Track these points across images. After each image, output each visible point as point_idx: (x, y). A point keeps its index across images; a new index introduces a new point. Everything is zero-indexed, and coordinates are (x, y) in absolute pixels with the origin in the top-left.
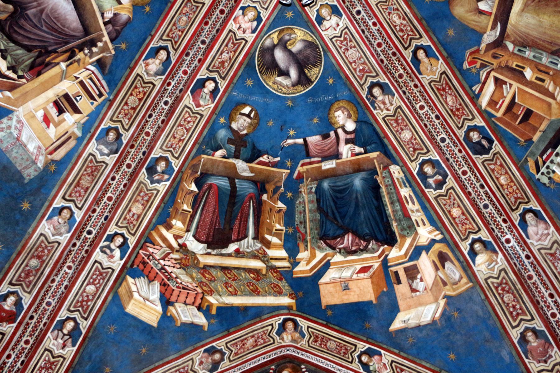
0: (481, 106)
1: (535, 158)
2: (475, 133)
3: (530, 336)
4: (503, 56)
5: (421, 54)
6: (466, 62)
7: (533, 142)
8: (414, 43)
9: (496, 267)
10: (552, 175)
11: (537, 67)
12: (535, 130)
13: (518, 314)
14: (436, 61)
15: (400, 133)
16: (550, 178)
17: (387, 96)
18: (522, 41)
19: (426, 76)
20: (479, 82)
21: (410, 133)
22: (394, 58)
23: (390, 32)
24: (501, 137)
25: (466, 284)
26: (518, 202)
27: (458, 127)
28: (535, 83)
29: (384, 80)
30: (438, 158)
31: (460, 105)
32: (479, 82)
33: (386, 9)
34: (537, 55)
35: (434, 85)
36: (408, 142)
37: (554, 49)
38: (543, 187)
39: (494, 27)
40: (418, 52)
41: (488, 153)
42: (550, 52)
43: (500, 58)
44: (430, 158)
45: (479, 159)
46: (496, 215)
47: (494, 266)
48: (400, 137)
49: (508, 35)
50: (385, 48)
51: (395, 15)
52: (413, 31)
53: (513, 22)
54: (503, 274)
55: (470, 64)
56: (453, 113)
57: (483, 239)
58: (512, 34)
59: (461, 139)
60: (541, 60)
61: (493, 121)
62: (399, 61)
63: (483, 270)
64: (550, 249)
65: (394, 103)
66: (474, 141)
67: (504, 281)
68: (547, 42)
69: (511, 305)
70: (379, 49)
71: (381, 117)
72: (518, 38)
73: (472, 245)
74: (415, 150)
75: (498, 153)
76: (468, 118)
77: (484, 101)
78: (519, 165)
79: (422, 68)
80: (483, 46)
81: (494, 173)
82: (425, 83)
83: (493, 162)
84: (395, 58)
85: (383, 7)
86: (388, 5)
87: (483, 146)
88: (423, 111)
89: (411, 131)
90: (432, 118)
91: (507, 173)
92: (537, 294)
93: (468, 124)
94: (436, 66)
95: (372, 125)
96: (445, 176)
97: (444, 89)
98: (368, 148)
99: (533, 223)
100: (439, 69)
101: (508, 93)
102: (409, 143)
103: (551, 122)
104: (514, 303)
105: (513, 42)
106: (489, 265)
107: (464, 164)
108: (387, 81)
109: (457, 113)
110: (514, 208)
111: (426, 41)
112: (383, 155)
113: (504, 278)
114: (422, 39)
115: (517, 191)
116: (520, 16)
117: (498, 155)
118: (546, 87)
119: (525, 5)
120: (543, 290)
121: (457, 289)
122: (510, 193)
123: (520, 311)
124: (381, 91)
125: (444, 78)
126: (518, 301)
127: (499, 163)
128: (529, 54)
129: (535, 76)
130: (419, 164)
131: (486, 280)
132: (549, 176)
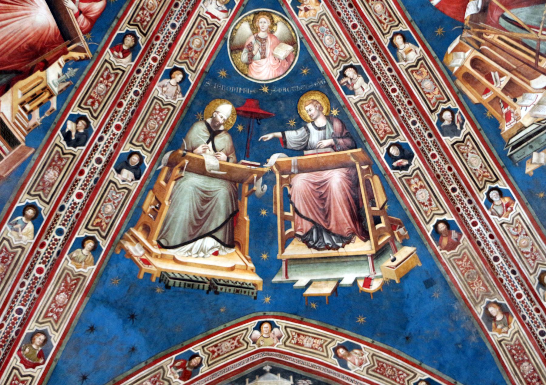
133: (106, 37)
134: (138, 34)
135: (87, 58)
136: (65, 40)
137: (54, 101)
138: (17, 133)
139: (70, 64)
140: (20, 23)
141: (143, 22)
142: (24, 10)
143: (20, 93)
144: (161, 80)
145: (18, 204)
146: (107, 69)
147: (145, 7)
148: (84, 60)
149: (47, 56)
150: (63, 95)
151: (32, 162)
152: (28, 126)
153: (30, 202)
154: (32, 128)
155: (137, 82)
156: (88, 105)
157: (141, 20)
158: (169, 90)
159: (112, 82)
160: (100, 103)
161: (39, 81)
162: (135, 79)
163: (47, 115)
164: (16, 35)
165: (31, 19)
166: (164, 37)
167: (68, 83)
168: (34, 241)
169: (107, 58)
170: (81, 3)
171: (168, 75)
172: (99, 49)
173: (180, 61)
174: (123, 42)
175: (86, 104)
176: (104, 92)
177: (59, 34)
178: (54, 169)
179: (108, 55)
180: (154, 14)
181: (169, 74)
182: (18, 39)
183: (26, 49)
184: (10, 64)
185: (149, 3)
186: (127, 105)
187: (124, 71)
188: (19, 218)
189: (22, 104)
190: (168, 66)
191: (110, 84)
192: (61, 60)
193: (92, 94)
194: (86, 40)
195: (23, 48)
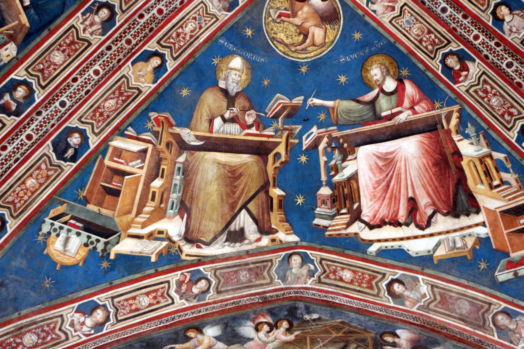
0: (111, 141)
1: (68, 212)
2: (80, 139)
4: (171, 153)
5: (156, 62)
6: (157, 115)
7: (86, 206)
8: (166, 52)
10: (53, 234)
11: (165, 191)
12: (100, 204)
14: (151, 81)
15: (58, 50)
16: (49, 233)
17: (100, 27)
18: (189, 169)
19: (132, 70)
20: (138, 133)
21: (61, 62)
22: (147, 30)
23: (174, 21)
24: (82, 169)
26: (9, 206)
27: (81, 117)
28: (149, 192)
29: (119, 21)
30: (38, 101)
31: (108, 116)
32: (138, 133)
33: (199, 15)
34: (178, 187)
35: (124, 82)
36: (50, 62)
37: (187, 203)
38: (37, 228)
39: (198, 138)
40: (158, 58)
41: (58, 158)
42: (183, 200)
43: (168, 150)
44: (35, 92)
45: (47, 148)
48: (53, 50)
49: (193, 154)
50: (157, 18)
51: (194, 25)
52: (179, 48)
53: (206, 157)
55: (156, 119)
56: (96, 110)
58: (195, 158)
59: (67, 124)
60: (174, 192)
61: (98, 157)
62: (144, 37)
65: (94, 36)
66: (68, 139)
68: (193, 194)
70: (155, 11)
71: (74, 23)
72: (192, 165)
74: (42, 71)
75: (63, 170)
76: (95, 128)
77: (118, 143)
78: (54, 196)
79: (140, 64)
80: (177, 130)
81: (36, 170)
82: (124, 70)
83: (49, 167)
84: (148, 32)
85: (201, 10)
86: (204, 16)
87: (65, 151)
88: (92, 75)
89: (64, 63)
90: (86, 87)
91: (41, 185)
93: (87, 129)
94: (146, 81)
95: (62, 13)
96: (17, 114)
97: (121, 94)
98: (32, 11)
100: (143, 86)
101: (133, 167)
102: (49, 63)
103: (111, 218)
105: (186, 160)
107: (39, 134)
108: (118, 24)
109: (97, 114)
111: (171, 65)
112: (27, 31)
114: (172, 60)
115: (22, 202)
116: (214, 162)
117: (59, 171)
118: (148, 204)
119: (225, 165)
122: (18, 194)
124: (106, 18)
125: (135, 93)
127: (50, 173)
128: (178, 179)
129: (156, 190)
130: (25, 79)
132: (52, 231)
133: (442, 86)
134: (447, 50)
135: (460, 111)
136: (437, 129)
137: (497, 155)
138: (520, 201)
139: (462, 130)
140: (412, 168)
141: (434, 42)
142: (401, 161)
143: (480, 186)
144: (503, 32)
146: (476, 92)
147: (419, 38)
148: (460, 115)
149: (449, 150)
150: (493, 144)
152: (516, 187)
154: (520, 184)
155: (498, 62)
156: (511, 120)
157: (432, 45)
158: (516, 25)
159: (492, 88)
160: (512, 106)
161: (472, 164)
162: (494, 63)
163: (509, 166)
164: (422, 175)
165: (410, 158)
166: (454, 23)
167: (481, 136)
169: (464, 89)
170: (404, 106)
171: (500, 23)
172: (453, 96)
173: (486, 6)
174: (451, 69)
175: (509, 122)
176: (501, 99)
177: (429, 133)
179: (461, 88)
180: (428, 29)
181: (499, 21)
182: (427, 175)
183: (437, 169)
184: (448, 189)
185: (416, 33)
186: (520, 78)
187: (484, 73)
189: (491, 187)
190: (489, 21)
191: (494, 91)
192: (456, 138)
193: (500, 113)
194: (441, 108)
195: (436, 171)
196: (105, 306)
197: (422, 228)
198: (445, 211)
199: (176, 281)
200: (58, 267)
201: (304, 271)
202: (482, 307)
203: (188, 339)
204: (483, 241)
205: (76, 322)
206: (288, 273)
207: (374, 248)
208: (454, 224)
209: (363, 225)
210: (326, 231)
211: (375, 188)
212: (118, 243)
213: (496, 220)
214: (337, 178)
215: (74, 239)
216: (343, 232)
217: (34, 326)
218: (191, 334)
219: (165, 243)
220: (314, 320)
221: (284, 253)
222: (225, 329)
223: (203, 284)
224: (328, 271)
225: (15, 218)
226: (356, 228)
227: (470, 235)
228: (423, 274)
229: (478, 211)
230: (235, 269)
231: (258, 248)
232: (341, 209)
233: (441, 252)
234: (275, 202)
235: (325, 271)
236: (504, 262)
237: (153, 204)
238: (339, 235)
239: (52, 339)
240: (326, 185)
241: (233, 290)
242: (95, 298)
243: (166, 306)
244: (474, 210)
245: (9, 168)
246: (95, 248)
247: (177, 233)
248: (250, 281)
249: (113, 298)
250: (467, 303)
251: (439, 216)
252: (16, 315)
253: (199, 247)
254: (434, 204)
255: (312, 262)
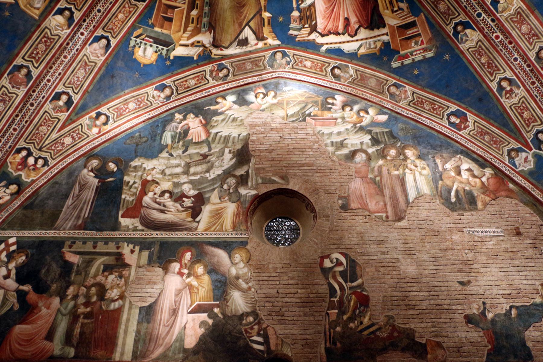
3: (24, 71)
9: (60, 31)
10: (137, 46)
11: (200, 17)
12: (162, 27)
13: (34, 58)
16: (135, 46)
25: (36, 14)
28: (190, 18)
37: (213, 24)
38: (127, 43)
46: (96, 20)
47: (59, 30)
54: (57, 38)
57: (74, 15)
60: (205, 17)
63: (52, 23)
64: (90, 62)
67: (52, 40)
69: (38, 50)
73: (66, 9)
75: (138, 7)
91: (127, 17)
92: (56, 65)
99: (101, 45)
101: (179, 3)
104: (40, 52)
106: (58, 26)
110: (105, 29)
113: (54, 39)
115: (117, 28)
120: (61, 68)
121: (27, 8)
123: (37, 58)
126: (43, 54)
127: (131, 9)
128: (206, 9)
131: (46, 27)
143: (386, 11)
145: (451, 34)
151: (429, 16)
153: (453, 26)
168: (479, 32)
178: (439, 4)
184: (368, 12)
188: (460, 36)
196: (170, 86)
197: (352, 37)
198: (365, 26)
199: (210, 71)
200: (142, 66)
201: (284, 61)
202: (383, 82)
203: (218, 103)
204: (386, 45)
205: (155, 96)
206: (275, 63)
207: (324, 48)
208: (370, 34)
209: (318, 34)
210: (296, 38)
211: (325, 12)
212: (174, 49)
213: (394, 31)
214: (302, 6)
215: (149, 48)
216: (306, 38)
217: (133, 99)
218: (219, 100)
219: (201, 49)
220: (289, 91)
221: (272, 52)
222: (239, 97)
223: (225, 71)
224: (297, 62)
225: (114, 38)
226: (313, 36)
227: (379, 41)
228: (351, 63)
229: (384, 26)
230: (243, 62)
231: (257, 49)
232: (305, 24)
233: (362, 51)
234: (266, 21)
235: (296, 62)
236: (396, 56)
237: (194, 25)
238: (304, 40)
239: (144, 105)
240: (296, 10)
241: (242, 74)
242: (164, 82)
243: (204, 84)
244: (383, 25)
245: (107, 8)
246: (161, 53)
247: (208, 42)
248: (252, 68)
249: (174, 81)
250: (375, 80)
251: (362, 30)
252: (123, 93)
253: (221, 50)
254: (359, 22)
255: (288, 56)
